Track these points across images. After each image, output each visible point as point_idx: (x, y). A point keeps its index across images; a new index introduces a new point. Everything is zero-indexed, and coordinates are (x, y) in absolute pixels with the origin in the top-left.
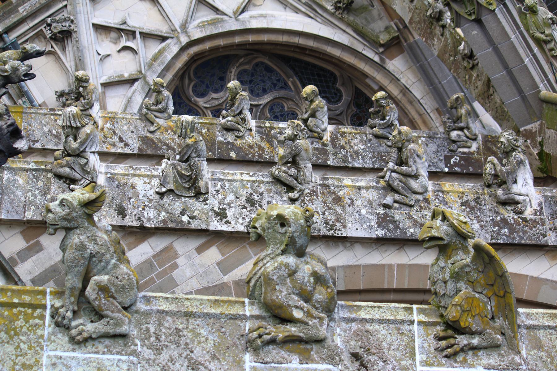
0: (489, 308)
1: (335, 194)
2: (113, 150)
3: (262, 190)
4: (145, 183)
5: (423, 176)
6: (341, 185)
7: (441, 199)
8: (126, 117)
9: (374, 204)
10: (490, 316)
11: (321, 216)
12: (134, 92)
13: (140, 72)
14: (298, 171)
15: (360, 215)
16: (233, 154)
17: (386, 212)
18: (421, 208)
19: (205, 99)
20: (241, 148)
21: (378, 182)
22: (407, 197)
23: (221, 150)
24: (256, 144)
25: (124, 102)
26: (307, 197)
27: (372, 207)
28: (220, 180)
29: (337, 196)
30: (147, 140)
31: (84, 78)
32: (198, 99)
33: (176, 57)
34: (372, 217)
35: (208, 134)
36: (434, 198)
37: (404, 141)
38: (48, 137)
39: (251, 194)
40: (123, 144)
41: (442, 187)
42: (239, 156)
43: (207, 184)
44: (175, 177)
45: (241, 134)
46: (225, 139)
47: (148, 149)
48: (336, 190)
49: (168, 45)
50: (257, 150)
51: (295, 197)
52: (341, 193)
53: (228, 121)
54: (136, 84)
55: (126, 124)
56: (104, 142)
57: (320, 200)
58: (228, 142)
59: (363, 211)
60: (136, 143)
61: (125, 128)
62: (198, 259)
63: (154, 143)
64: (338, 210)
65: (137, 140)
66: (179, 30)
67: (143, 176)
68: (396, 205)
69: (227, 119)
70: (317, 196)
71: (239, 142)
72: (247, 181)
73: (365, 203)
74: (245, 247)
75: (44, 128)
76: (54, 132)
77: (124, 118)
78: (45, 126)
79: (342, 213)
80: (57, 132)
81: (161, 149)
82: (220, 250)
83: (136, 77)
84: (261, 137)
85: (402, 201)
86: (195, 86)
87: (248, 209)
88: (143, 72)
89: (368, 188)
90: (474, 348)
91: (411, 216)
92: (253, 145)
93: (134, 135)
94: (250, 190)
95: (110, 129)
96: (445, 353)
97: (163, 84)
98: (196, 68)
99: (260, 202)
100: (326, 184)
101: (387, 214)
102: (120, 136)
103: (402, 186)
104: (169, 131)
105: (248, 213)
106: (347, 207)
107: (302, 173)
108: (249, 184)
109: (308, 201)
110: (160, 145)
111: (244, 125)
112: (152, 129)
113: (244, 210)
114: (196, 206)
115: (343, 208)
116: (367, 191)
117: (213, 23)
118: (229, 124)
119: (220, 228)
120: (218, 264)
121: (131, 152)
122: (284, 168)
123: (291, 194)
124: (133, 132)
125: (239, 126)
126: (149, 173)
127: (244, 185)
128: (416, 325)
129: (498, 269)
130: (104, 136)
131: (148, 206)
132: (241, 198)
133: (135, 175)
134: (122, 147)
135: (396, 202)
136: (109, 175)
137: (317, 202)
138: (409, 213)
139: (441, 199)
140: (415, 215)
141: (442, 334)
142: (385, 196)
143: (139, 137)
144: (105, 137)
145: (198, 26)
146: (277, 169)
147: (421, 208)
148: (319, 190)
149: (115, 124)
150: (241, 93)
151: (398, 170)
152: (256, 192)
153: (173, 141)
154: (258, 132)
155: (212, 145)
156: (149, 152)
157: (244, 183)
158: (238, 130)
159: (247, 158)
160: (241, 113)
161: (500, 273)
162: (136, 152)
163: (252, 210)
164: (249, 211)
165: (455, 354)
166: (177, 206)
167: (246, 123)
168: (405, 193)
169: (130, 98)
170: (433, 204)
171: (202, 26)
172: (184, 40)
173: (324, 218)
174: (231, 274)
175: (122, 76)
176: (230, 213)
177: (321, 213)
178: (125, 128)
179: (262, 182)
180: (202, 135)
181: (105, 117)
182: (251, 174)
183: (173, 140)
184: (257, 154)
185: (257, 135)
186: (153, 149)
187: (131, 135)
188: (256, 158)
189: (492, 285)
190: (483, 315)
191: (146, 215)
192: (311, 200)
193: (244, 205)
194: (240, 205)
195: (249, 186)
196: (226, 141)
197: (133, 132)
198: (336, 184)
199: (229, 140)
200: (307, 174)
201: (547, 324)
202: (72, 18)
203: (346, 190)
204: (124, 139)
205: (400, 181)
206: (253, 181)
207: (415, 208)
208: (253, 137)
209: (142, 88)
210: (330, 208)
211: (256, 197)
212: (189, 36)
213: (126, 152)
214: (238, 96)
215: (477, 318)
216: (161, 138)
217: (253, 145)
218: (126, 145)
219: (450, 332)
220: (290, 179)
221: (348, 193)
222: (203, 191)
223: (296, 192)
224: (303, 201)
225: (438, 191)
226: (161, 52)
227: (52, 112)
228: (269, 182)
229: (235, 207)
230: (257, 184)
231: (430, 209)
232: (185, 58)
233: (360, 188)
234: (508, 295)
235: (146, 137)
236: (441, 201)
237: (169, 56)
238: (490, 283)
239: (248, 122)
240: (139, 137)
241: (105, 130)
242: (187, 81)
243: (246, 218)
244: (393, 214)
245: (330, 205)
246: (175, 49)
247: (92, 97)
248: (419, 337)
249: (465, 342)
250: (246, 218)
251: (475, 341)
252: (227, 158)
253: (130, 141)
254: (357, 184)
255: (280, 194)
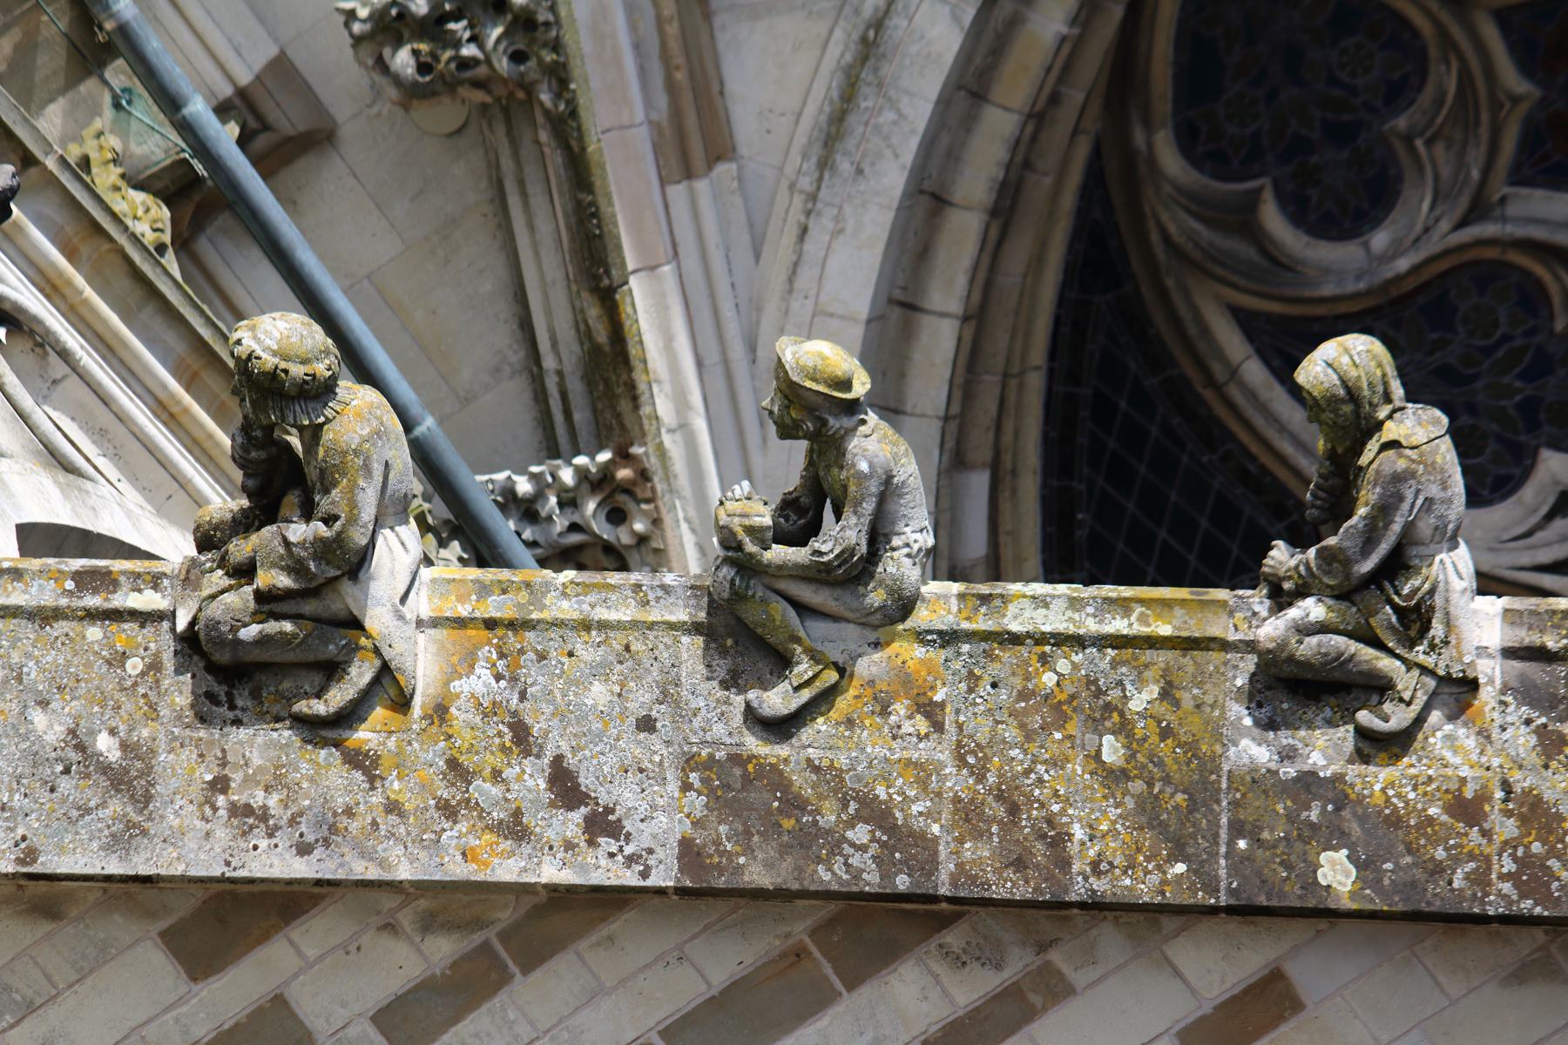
2: (508, 868)
8: (602, 614)
20: (1395, 821)
23: (1257, 841)
24: (1507, 787)
25: (840, 49)
30: (747, 780)
31: (298, 371)
35: (1171, 717)
38: (65, 785)
40: (578, 816)
42: (1376, 883)
45: (1397, 717)
46: (1287, 755)
47: (749, 850)
50: (1508, 828)
53: (1305, 629)
55: (600, 671)
56: (449, 811)
58: (1308, 782)
60: (673, 808)
61: (598, 693)
63: (795, 804)
65: (673, 787)
69: (1293, 613)
71: (1378, 779)
75: (39, 718)
76: (105, 744)
77: (586, 626)
78: (44, 704)
80: (124, 746)
81: (837, 844)
84: (1541, 731)
92: (1483, 797)
93: (656, 749)
95: (490, 711)
97: (846, 384)
102: (558, 760)
104: (900, 708)
110: (829, 818)
111: (1419, 654)
112: (777, 700)
118: (1310, 646)
121: (631, 878)
124: (646, 724)
125: (1386, 664)
130: (453, 764)
134: (569, 846)
143: (689, 762)
144: (457, 770)
149: (531, 673)
150: (1391, 431)
153: (923, 784)
154: (1527, 693)
155: (1193, 806)
156: (757, 875)
158: (1380, 688)
159: (1435, 897)
160: (1397, 564)
162: (663, 877)
167: (1437, 630)
169: (878, 24)
178: (598, 693)
180: (1124, 729)
181: (460, 623)
183: (922, 773)
184: (1509, 866)
185: (1517, 712)
186: (784, 850)
187: (633, 746)
188: (1502, 896)
196: (1289, 771)
197: (646, 724)
199: (1316, 759)
204: (586, 781)
208: (1484, 735)
213: (597, 878)
214: (1372, 446)
216: (843, 761)
217: (1483, 797)
218: (602, 825)
227: (93, 601)
235: (736, 759)
239: (1448, 624)
240: (689, 762)
241: (461, 715)
247: (353, 505)
252: (1293, 896)
253: (625, 796)
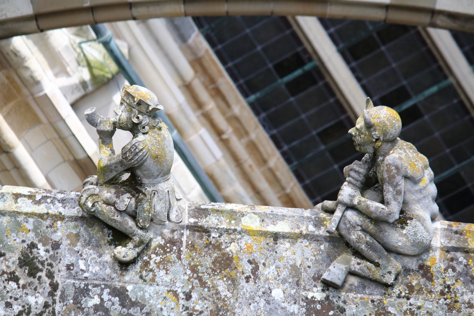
1: (220, 249)
3: (57, 236)
5: (420, 219)
6: (235, 230)
7: (459, 268)
9: (304, 274)
11: (182, 302)
14: (138, 201)
15: (268, 302)
17: (327, 298)
18: (411, 288)
21: (319, 223)
22: (377, 265)
26: (157, 254)
27: (298, 284)
29: (224, 254)
36: (443, 267)
37: (379, 144)
39: (33, 246)
41: (466, 241)
48: (222, 239)
51: (127, 259)
52: (233, 248)
57: (185, 262)
59: (277, 294)
64: (220, 289)
68: (353, 280)
70: (180, 252)
72: (26, 214)
73: (285, 273)
79: (229, 295)
85: (367, 273)
87: (21, 282)
91: (384, 308)
94: (31, 237)
99: (50, 265)
100: (201, 227)
101: (331, 302)
103: (367, 243)
105: (20, 293)
106: (243, 282)
107: (146, 206)
108: (31, 220)
109: (158, 265)
113: (13, 285)
115: (234, 282)
116: (293, 243)
123: (119, 248)
127: (19, 224)
132: (7, 256)
135: (351, 273)
137: (177, 268)
138: (381, 301)
139: (459, 268)
140: (393, 306)
142: (330, 258)
146: (92, 195)
147: (411, 288)
148: (184, 239)
151: (361, 207)
152: (45, 240)
157: (20, 218)
163: (30, 284)
164: (24, 287)
168: (374, 256)
170: (441, 281)
173: (187, 308)
177: (182, 295)
179: (60, 217)
182: (38, 197)
192: (164, 264)
193: (14, 272)
194: (4, 273)
195: (30, 226)
198: (224, 226)
200: (158, 208)
203: (246, 240)
205: (364, 230)
206: (41, 216)
207: (396, 290)
210: (203, 284)
211: (42, 253)
220: (118, 218)
221: (249, 247)
223: (130, 245)
224: (147, 264)
225: (456, 249)
228: (75, 219)
230: (48, 222)
231: (431, 292)
233: (276, 237)
236: (460, 274)
243: (14, 303)
244: (345, 302)
245: (206, 277)
250: (14, 303)
254: (272, 228)
255: (97, 246)
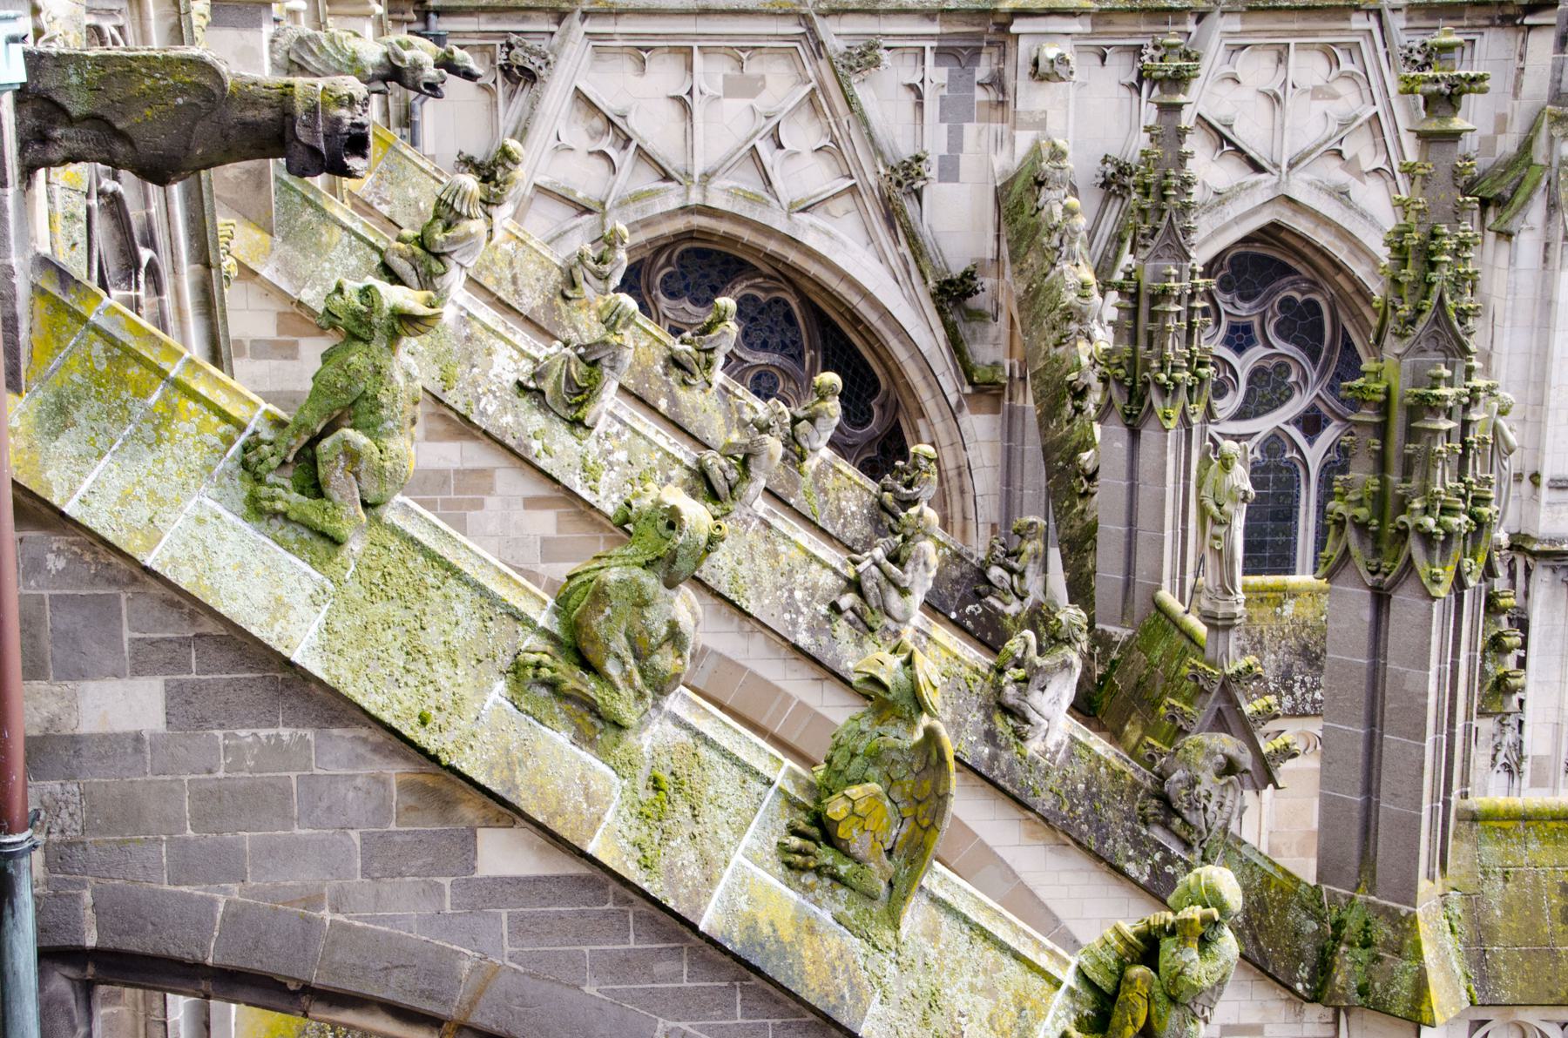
0: (894, 832)
3: (672, 473)
4: (511, 357)
10: (888, 846)
12: (576, 227)
13: (603, 204)
14: (741, 480)
16: (663, 405)
19: (673, 303)
21: (845, 565)
28: (621, 422)
32: (661, 296)
33: (669, 215)
34: (805, 610)
43: (599, 414)
44: (559, 376)
45: (692, 382)
49: (667, 190)
52: (782, 548)
54: (587, 217)
62: (519, 513)
66: (696, 178)
67: (514, 346)
68: (851, 615)
74: (598, 539)
82: (559, 522)
83: (592, 206)
86: (670, 275)
88: (608, 206)
89: (825, 566)
90: (836, 878)
96: (790, 858)
98: (687, 251)
114: (562, 438)
117: (754, 199)
118: (684, 356)
119: (578, 490)
120: (544, 541)
122: (723, 462)
126: (525, 347)
128: (772, 791)
129: (942, 785)
131: (493, 393)
133: (502, 338)
136: (463, 314)
141: (802, 826)
142: (843, 592)
145: (727, 191)
158: (693, 375)
160: (711, 350)
161: (941, 792)
165: (804, 869)
166: (537, 421)
169: (565, 232)
171: (733, 193)
172: (695, 198)
174: (553, 566)
175: (573, 192)
176: (606, 479)
178: (531, 267)
179: (680, 462)
189: (919, 802)
190: (879, 837)
191: (482, 405)
201: (964, 911)
202: (551, 57)
206: (668, 454)
209: (592, 229)
212: (705, 197)
215: (869, 835)
218: (517, 292)
219: (815, 831)
220: (722, 482)
222: (587, 422)
226: (652, 193)
229: (620, 474)
232: (680, 224)
234: (933, 831)
237: (658, 207)
238: (918, 797)
242: (662, 260)
246: (674, 203)
248: (767, 810)
249: (828, 860)
251: (844, 869)
253: (527, 291)
